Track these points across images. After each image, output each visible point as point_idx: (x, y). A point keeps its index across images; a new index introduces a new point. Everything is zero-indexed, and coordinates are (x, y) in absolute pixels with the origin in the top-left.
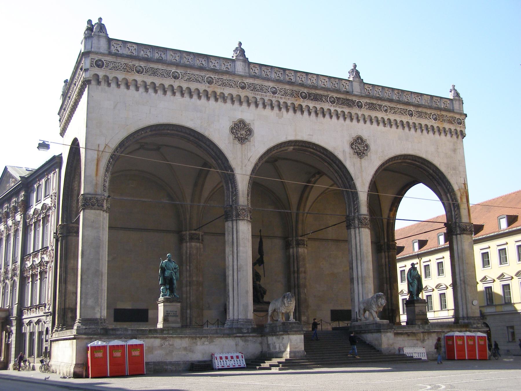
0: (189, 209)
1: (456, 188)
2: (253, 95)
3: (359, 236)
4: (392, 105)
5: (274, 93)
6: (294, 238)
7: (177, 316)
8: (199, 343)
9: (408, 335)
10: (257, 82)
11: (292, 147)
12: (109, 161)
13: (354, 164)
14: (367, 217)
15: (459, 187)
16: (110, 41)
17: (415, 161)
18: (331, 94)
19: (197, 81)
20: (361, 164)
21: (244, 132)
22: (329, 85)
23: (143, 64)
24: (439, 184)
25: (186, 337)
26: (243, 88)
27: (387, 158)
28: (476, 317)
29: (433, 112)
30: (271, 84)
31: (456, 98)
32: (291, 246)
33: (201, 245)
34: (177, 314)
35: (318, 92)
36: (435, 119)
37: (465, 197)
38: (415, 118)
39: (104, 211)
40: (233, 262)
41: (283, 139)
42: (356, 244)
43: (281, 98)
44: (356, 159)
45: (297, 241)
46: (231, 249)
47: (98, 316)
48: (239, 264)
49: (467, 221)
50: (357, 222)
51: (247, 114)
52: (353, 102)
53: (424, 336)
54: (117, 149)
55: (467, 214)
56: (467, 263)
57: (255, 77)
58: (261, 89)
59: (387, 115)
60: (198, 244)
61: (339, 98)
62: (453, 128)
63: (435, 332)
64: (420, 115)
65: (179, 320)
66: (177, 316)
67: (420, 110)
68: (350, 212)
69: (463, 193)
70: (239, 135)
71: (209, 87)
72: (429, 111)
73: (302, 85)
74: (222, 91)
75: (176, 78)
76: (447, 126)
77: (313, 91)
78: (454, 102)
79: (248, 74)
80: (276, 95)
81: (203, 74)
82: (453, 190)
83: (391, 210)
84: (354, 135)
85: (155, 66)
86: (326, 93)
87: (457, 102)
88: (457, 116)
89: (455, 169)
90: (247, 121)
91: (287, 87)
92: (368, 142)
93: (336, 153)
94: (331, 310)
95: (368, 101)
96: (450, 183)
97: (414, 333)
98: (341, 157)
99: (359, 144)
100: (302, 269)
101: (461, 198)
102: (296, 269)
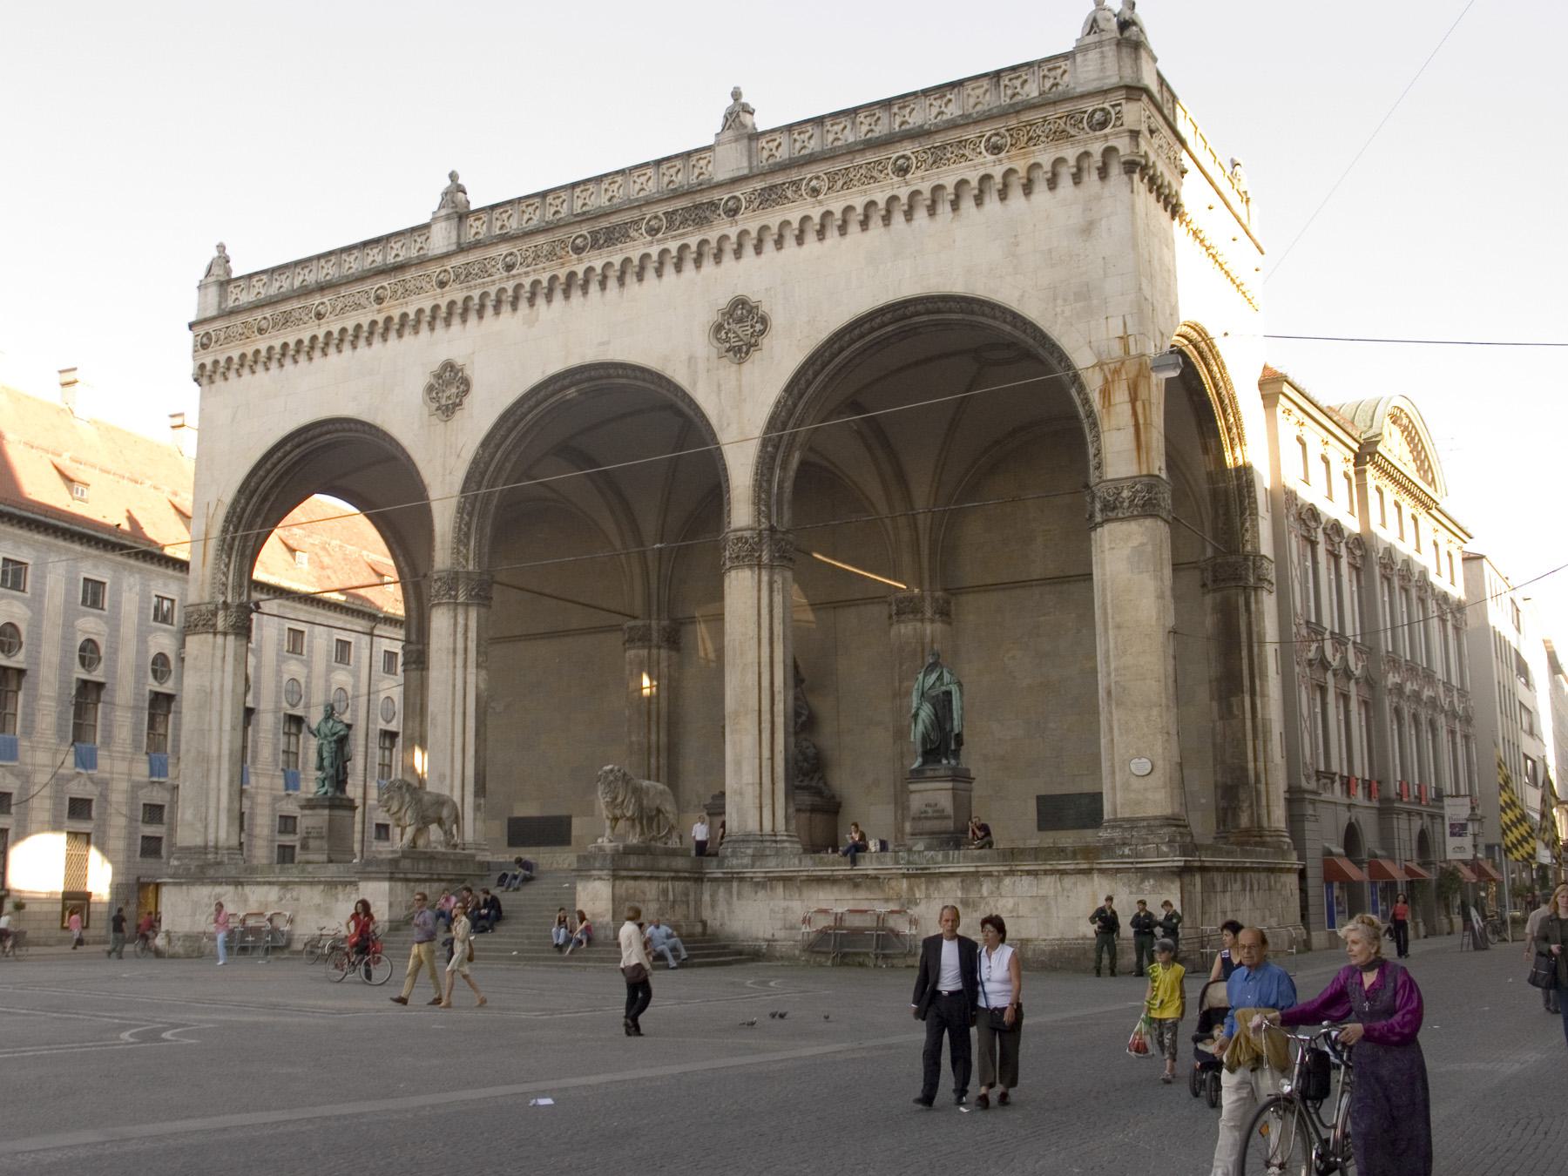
1: (1082, 359)
2: (465, 294)
4: (839, 165)
5: (509, 267)
8: (340, 896)
9: (856, 886)
10: (472, 257)
11: (573, 389)
12: (225, 530)
13: (719, 386)
14: (747, 534)
15: (1099, 355)
16: (225, 283)
17: (939, 311)
18: (649, 212)
19: (358, 306)
20: (739, 380)
21: (454, 390)
22: (651, 185)
23: (268, 312)
25: (320, 882)
26: (442, 284)
27: (824, 335)
28: (1143, 819)
29: (988, 129)
30: (504, 249)
31: (1093, 38)
33: (664, 653)
35: (615, 219)
36: (996, 149)
37: (1124, 385)
38: (920, 173)
39: (215, 634)
41: (535, 378)
43: (527, 273)
44: (728, 372)
47: (199, 841)
49: (1132, 470)
51: (454, 343)
52: (713, 205)
53: (911, 889)
54: (236, 502)
55: (1133, 445)
56: (1118, 627)
57: (477, 245)
58: (485, 272)
59: (820, 202)
60: (645, 652)
61: (674, 212)
62: (1070, 153)
63: (952, 874)
64: (938, 157)
67: (938, 140)
69: (1117, 372)
70: (443, 402)
71: (379, 311)
72: (971, 134)
73: (585, 217)
74: (404, 310)
75: (319, 316)
76: (1045, 157)
77: (604, 223)
78: (1079, 58)
79: (454, 247)
80: (514, 272)
81: (366, 286)
83: (1206, 450)
84: (724, 302)
85: (287, 307)
86: (636, 214)
87: (1093, 55)
88: (1089, 106)
89: (1084, 294)
90: (459, 361)
91: (541, 239)
92: (764, 308)
93: (668, 373)
94: (1038, 798)
95: (759, 185)
97: (876, 878)
98: (680, 377)
99: (740, 320)
101: (1106, 393)
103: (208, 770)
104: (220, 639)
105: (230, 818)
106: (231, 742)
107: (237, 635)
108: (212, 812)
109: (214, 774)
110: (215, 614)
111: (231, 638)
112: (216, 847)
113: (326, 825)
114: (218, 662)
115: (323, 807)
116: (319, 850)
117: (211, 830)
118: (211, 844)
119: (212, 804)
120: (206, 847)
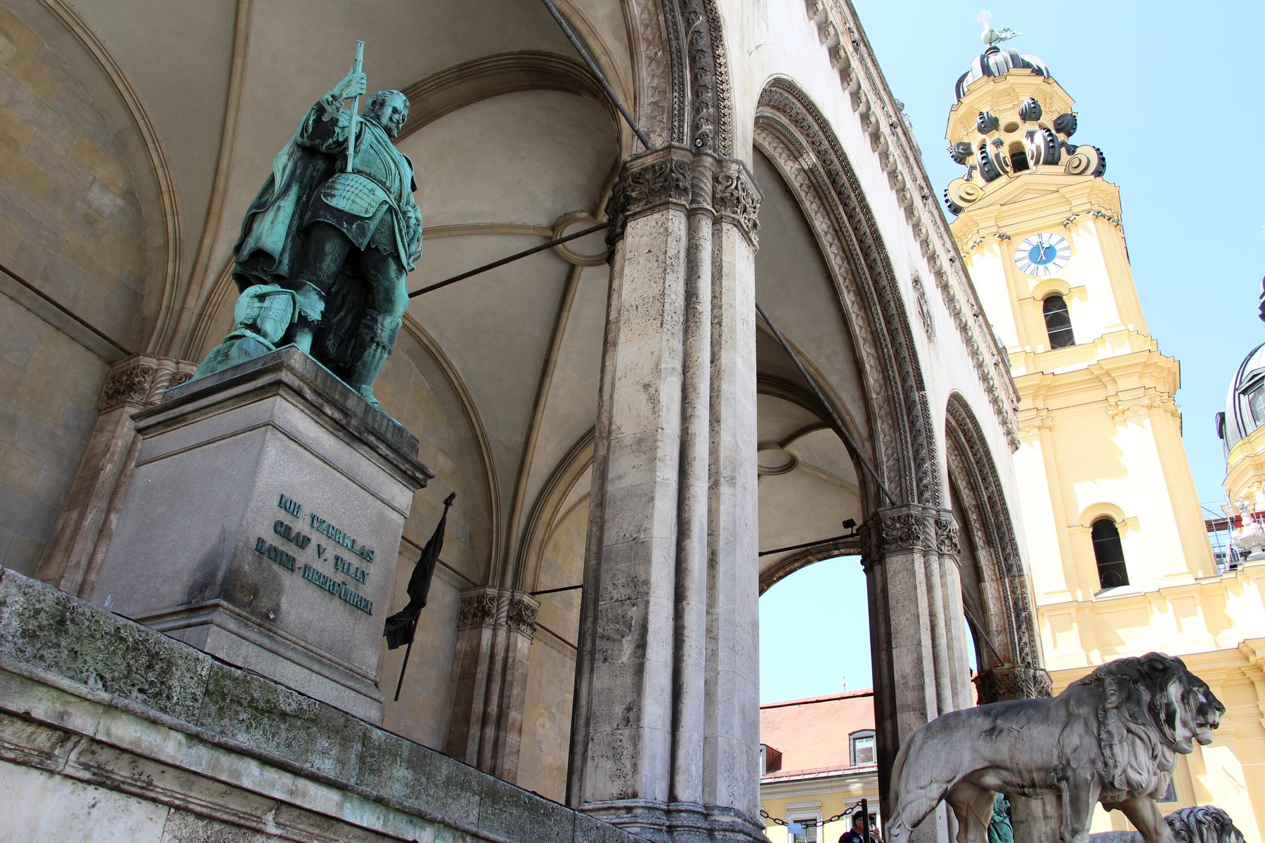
0: (211, 278)
3: (944, 585)
6: (508, 594)
24: (989, 542)
32: (489, 621)
34: (368, 590)
40: (685, 418)
42: (932, 615)
45: (512, 602)
46: (678, 345)
48: (725, 438)
50: (932, 530)
66: (363, 607)
68: (904, 492)
82: (1020, 570)
96: (1016, 549)
100: (513, 714)
102: (493, 708)
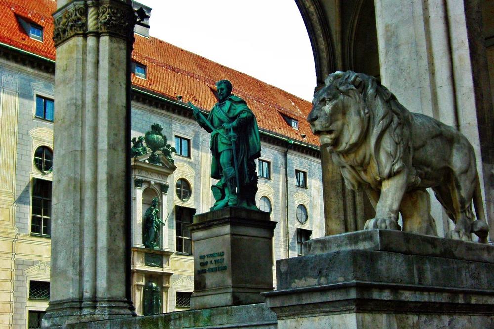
7: (224, 269)
39: (85, 36)
65: (229, 281)
66: (224, 269)
103: (82, 201)
104: (91, 41)
105: (111, 261)
106: (110, 165)
107: (112, 35)
108: (87, 253)
109: (88, 204)
110: (85, 13)
111: (105, 39)
112: (94, 300)
113: (226, 249)
114: (90, 68)
115: (222, 222)
116: (219, 289)
117: (87, 277)
118: (87, 295)
119: (88, 243)
120: (81, 300)
